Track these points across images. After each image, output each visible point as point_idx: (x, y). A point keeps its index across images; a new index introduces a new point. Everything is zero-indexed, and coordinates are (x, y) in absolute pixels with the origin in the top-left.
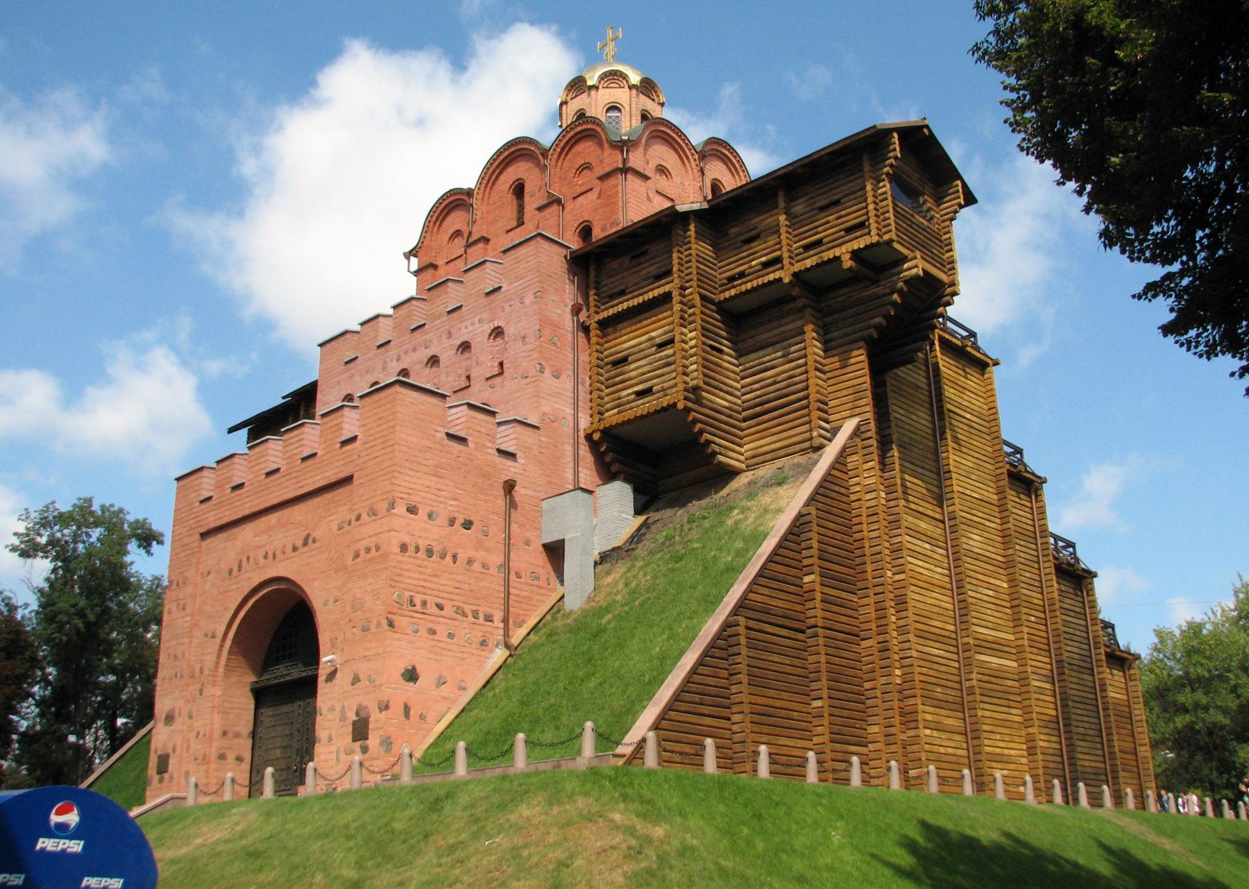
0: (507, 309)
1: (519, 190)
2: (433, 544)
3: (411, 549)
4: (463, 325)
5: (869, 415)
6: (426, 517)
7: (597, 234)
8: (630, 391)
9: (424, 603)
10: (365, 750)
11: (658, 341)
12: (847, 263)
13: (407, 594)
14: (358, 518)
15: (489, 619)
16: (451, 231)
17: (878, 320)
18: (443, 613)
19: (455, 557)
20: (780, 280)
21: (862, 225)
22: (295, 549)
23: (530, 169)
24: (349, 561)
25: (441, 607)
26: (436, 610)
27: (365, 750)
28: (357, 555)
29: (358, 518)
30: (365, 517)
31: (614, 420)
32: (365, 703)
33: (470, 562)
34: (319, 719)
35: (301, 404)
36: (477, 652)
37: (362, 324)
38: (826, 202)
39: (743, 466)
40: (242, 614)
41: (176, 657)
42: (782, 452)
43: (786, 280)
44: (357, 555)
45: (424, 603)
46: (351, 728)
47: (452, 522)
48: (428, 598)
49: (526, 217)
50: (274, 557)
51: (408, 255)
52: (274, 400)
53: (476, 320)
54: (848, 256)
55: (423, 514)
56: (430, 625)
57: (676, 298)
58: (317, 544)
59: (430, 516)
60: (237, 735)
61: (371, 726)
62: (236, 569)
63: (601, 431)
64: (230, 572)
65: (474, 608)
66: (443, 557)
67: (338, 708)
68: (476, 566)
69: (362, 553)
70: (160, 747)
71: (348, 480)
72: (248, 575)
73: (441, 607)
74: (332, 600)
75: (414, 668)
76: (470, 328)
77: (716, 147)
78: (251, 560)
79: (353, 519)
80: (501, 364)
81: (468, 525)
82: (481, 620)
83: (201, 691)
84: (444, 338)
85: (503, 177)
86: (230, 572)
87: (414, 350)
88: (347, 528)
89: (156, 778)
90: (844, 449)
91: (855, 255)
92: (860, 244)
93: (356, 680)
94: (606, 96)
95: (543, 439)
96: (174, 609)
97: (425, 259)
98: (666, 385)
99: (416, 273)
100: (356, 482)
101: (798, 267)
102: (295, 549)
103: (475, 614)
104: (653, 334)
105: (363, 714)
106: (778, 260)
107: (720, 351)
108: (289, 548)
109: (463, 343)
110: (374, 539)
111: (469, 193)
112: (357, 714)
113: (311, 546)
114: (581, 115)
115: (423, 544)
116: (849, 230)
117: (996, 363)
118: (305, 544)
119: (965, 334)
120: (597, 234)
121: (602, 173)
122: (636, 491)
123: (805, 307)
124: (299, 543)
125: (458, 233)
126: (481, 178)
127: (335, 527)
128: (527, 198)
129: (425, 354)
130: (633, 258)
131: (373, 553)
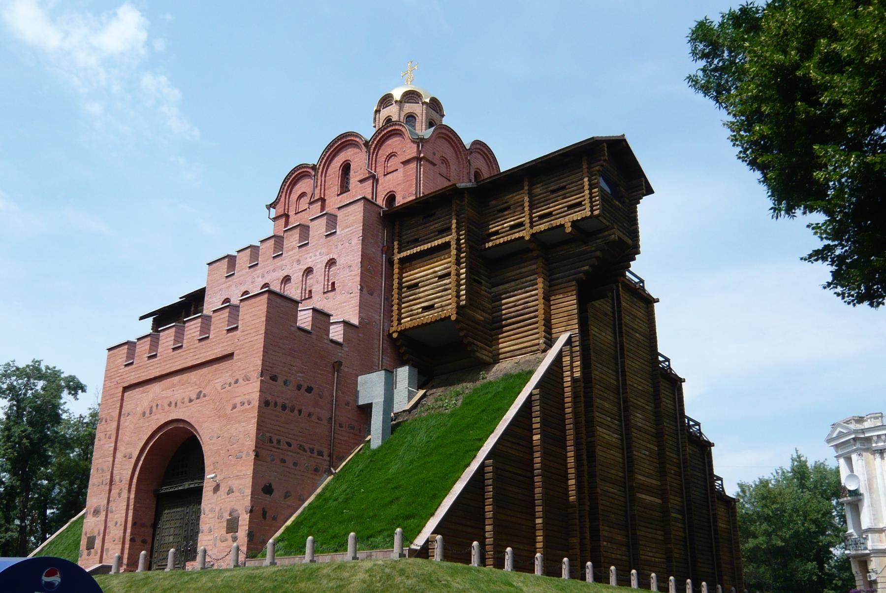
0: (340, 247)
1: (346, 168)
2: (287, 402)
3: (272, 404)
5: (577, 331)
6: (282, 384)
7: (399, 201)
8: (419, 306)
9: (279, 442)
10: (235, 539)
11: (439, 273)
12: (569, 229)
13: (268, 434)
14: (236, 382)
15: (320, 454)
16: (299, 193)
17: (586, 268)
18: (291, 449)
19: (300, 412)
20: (523, 237)
21: (579, 204)
22: (191, 401)
23: (355, 153)
24: (229, 411)
25: (289, 444)
26: (286, 447)
27: (235, 539)
28: (234, 407)
29: (236, 382)
30: (241, 381)
31: (408, 326)
32: (236, 507)
33: (310, 415)
34: (202, 516)
35: (193, 302)
36: (311, 476)
37: (238, 252)
39: (492, 360)
41: (103, 470)
42: (518, 352)
43: (527, 238)
44: (234, 407)
45: (279, 442)
46: (225, 524)
47: (299, 387)
48: (281, 438)
49: (351, 187)
50: (176, 404)
51: (269, 207)
52: (173, 298)
53: (318, 253)
54: (570, 224)
55: (280, 381)
56: (282, 457)
57: (453, 244)
59: (285, 383)
60: (143, 525)
61: (240, 523)
62: (148, 412)
63: (399, 332)
64: (144, 414)
65: (311, 446)
66: (292, 411)
68: (314, 418)
69: (238, 405)
70: (89, 531)
71: (230, 356)
72: (156, 417)
73: (289, 444)
74: (215, 435)
75: (270, 484)
76: (313, 258)
77: (478, 146)
79: (233, 382)
80: (333, 284)
81: (309, 390)
82: (315, 455)
84: (295, 264)
85: (336, 159)
87: (274, 270)
88: (228, 388)
89: (86, 552)
90: (561, 351)
91: (574, 223)
92: (577, 216)
93: (230, 491)
94: (409, 108)
95: (360, 335)
97: (281, 209)
98: (443, 303)
99: (275, 219)
100: (235, 357)
101: (536, 229)
102: (191, 401)
103: (312, 451)
104: (437, 269)
105: (235, 514)
106: (521, 224)
107: (480, 283)
108: (187, 400)
109: (308, 268)
110: (247, 397)
111: (314, 167)
112: (230, 515)
113: (203, 399)
114: (389, 120)
115: (280, 401)
116: (570, 207)
117: (658, 301)
118: (198, 398)
119: (637, 280)
120: (399, 201)
121: (404, 160)
122: (419, 373)
123: (537, 257)
124: (194, 397)
125: (303, 194)
126: (321, 158)
127: (219, 388)
128: (352, 173)
129: (282, 274)
131: (246, 406)
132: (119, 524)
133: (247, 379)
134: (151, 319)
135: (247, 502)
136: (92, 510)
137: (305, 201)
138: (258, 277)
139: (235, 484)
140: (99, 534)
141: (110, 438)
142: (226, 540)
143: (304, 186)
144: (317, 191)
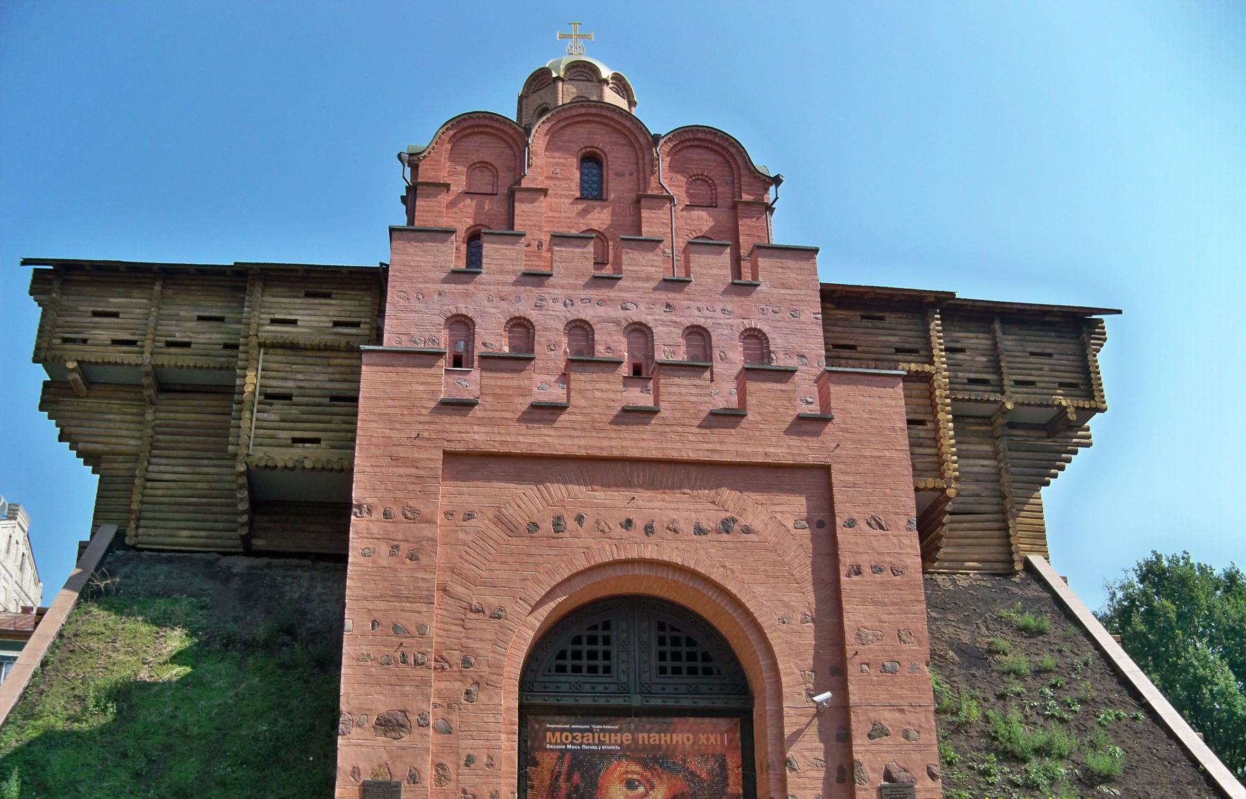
4: (694, 305)
14: (851, 523)
23: (616, 144)
38: (1038, 351)
50: (649, 530)
53: (719, 307)
58: (753, 537)
62: (547, 526)
69: (867, 570)
85: (567, 133)
118: (726, 526)
125: (483, 165)
130: (863, 317)
138: (555, 300)
139: (888, 718)
140: (414, 778)
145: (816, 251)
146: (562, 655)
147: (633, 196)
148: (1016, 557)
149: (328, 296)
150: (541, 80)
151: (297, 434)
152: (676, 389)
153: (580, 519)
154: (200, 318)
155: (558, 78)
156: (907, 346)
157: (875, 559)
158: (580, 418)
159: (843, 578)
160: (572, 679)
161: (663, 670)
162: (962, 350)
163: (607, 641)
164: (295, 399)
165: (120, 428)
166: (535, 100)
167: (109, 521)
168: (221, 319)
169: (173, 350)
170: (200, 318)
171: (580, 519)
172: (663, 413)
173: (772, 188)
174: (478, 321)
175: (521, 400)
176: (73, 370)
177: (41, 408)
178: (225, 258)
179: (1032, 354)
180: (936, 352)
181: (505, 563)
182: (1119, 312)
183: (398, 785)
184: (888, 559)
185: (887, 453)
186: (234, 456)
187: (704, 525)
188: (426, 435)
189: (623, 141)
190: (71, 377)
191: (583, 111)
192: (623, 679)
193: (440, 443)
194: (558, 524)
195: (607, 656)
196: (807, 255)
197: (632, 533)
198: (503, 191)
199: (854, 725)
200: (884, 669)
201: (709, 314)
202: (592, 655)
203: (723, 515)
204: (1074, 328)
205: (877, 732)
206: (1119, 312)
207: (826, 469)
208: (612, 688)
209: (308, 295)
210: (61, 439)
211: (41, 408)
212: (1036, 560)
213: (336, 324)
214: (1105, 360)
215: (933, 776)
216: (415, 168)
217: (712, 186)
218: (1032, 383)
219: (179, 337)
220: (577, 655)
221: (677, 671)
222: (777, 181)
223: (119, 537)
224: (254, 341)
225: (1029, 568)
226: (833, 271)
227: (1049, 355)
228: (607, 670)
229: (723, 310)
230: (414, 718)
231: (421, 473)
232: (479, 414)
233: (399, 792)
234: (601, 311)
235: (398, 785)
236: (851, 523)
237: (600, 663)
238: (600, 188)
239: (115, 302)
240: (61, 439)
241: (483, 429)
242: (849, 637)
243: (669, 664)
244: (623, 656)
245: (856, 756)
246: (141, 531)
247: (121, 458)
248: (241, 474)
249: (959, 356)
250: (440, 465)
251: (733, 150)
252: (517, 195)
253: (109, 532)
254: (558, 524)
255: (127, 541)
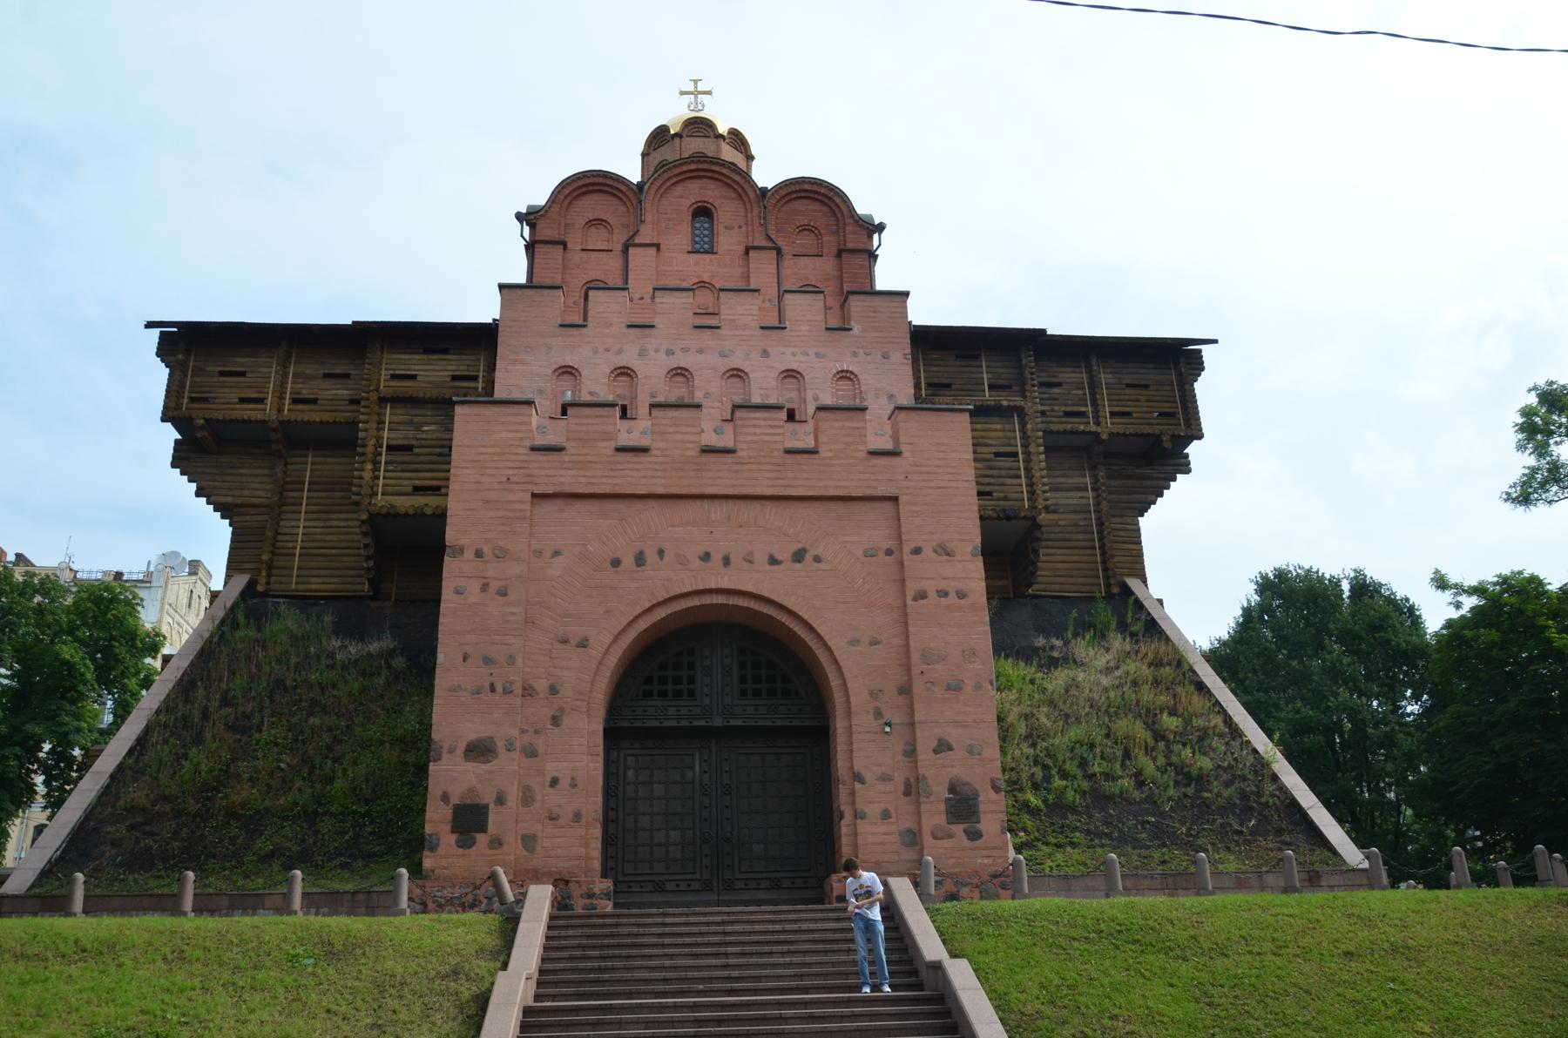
10: (974, 835)
14: (917, 551)
20: (1097, 434)
27: (974, 835)
30: (928, 552)
32: (966, 778)
40: (643, 625)
44: (921, 595)
46: (942, 807)
50: (727, 561)
51: (519, 217)
53: (812, 352)
58: (822, 566)
62: (628, 561)
64: (616, 563)
67: (899, 778)
69: (932, 595)
78: (666, 558)
83: (555, 721)
85: (679, 189)
86: (616, 563)
87: (700, 351)
89: (449, 840)
96: (474, 587)
102: (773, 561)
106: (1083, 414)
108: (761, 557)
112: (952, 789)
118: (799, 556)
124: (784, 552)
125: (598, 222)
130: (957, 357)
131: (952, 599)
132: (565, 782)
133: (945, 551)
134: (155, 333)
135: (995, 770)
136: (462, 746)
137: (597, 239)
138: (657, 351)
139: (953, 735)
140: (500, 800)
141: (503, 592)
142: (950, 836)
143: (593, 206)
144: (644, 229)
145: (906, 294)
146: (649, 681)
147: (742, 248)
148: (1112, 581)
149: (446, 352)
150: (659, 137)
151: (418, 483)
152: (752, 430)
153: (661, 553)
154: (326, 376)
155: (676, 135)
156: (1001, 382)
157: (943, 585)
158: (661, 459)
159: (909, 602)
160: (659, 703)
161: (743, 693)
162: (1059, 385)
163: (691, 666)
164: (416, 450)
165: (255, 484)
166: (657, 157)
167: (242, 571)
168: (347, 376)
169: (300, 407)
170: (326, 376)
171: (661, 553)
172: (740, 453)
173: (876, 236)
174: (584, 372)
175: (605, 444)
176: (201, 428)
177: (173, 465)
178: (345, 319)
179: (1128, 386)
180: (1028, 387)
181: (590, 596)
182: (1215, 341)
183: (486, 807)
184: (953, 583)
185: (954, 484)
186: (357, 504)
187: (778, 557)
188: (514, 479)
189: (731, 194)
190: (199, 434)
191: (693, 167)
192: (707, 701)
193: (529, 487)
194: (640, 559)
195: (691, 680)
196: (898, 298)
197: (709, 565)
198: (619, 247)
199: (919, 742)
200: (949, 688)
201: (803, 358)
202: (678, 680)
203: (796, 547)
204: (1171, 363)
205: (943, 747)
206: (1215, 341)
207: (895, 499)
208: (697, 711)
209: (427, 351)
210: (198, 494)
211: (173, 465)
212: (1134, 584)
213: (455, 378)
214: (1202, 387)
215: (997, 789)
216: (532, 226)
217: (819, 236)
218: (1128, 414)
219: (306, 393)
220: (663, 681)
221: (757, 693)
222: (880, 228)
223: (251, 585)
224: (374, 397)
225: (1127, 591)
226: (921, 313)
227: (1146, 386)
228: (691, 693)
229: (817, 355)
230: (500, 744)
231: (510, 514)
232: (567, 458)
233: (486, 814)
234: (700, 357)
235: (486, 807)
236: (917, 551)
237: (685, 687)
238: (711, 243)
239: (239, 362)
240: (198, 494)
241: (571, 473)
242: (915, 657)
243: (749, 686)
244: (707, 681)
245: (921, 771)
246: (273, 579)
247: (252, 511)
248: (363, 522)
249: (1056, 390)
250: (528, 506)
251: (838, 200)
252: (631, 250)
253: (241, 581)
254: (640, 559)
255: (260, 588)
